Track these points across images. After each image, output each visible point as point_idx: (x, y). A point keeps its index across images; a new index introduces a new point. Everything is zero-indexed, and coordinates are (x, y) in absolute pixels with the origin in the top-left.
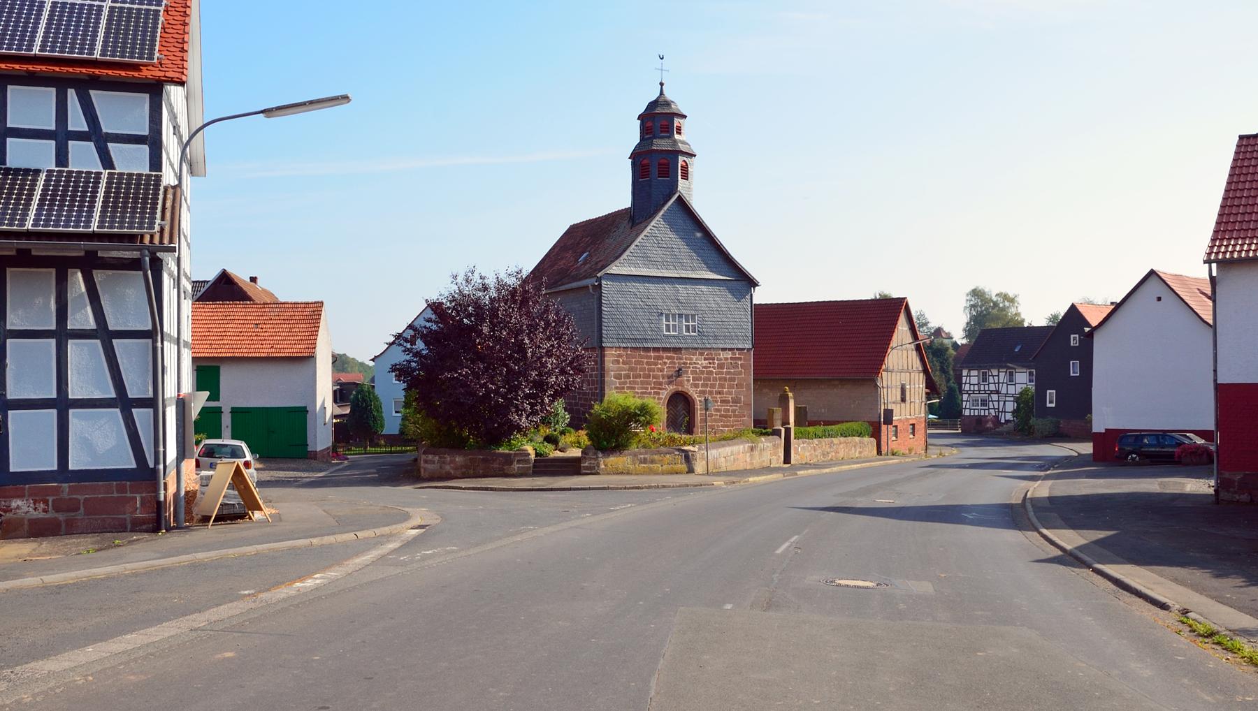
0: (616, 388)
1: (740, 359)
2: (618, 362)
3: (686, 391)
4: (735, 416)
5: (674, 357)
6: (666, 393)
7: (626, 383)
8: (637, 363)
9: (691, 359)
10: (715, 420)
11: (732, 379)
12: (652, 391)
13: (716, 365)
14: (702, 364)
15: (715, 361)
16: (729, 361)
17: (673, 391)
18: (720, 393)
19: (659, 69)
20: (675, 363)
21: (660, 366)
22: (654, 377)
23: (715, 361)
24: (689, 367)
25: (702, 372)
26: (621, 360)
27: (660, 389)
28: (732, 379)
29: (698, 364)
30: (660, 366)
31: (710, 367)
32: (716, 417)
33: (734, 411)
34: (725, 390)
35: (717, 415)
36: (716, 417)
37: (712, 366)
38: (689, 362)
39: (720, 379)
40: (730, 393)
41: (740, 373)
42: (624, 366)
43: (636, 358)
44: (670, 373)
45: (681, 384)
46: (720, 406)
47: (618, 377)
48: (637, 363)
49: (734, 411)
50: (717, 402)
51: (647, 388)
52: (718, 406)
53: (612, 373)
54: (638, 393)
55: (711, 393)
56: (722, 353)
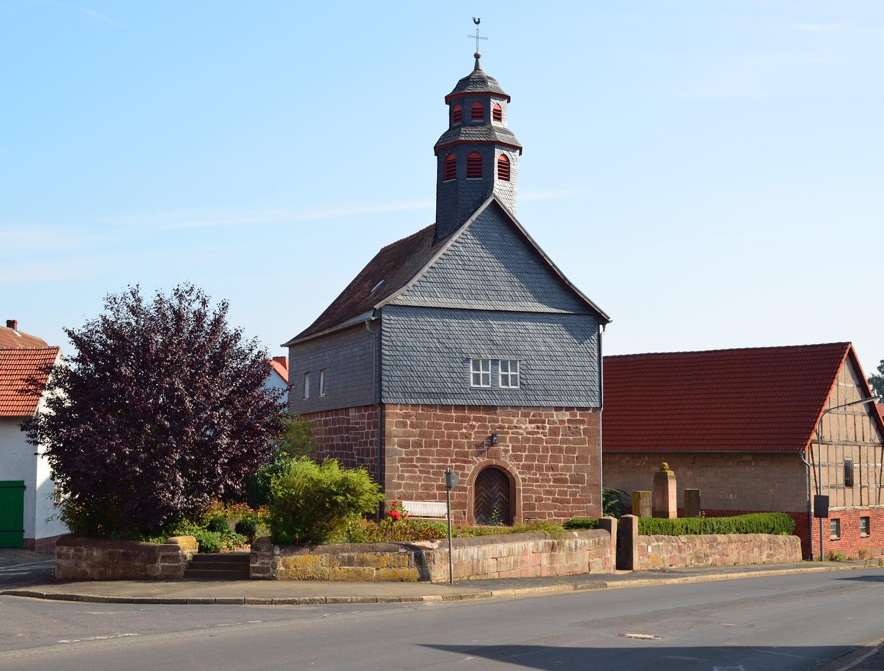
0: (401, 460)
1: (582, 422)
2: (404, 425)
3: (503, 465)
4: (575, 501)
5: (485, 418)
6: (473, 467)
7: (415, 453)
8: (432, 426)
9: (510, 422)
10: (546, 506)
11: (571, 450)
12: (454, 464)
13: (547, 431)
14: (527, 428)
15: (546, 425)
16: (566, 425)
17: (484, 465)
18: (552, 468)
19: (473, 37)
20: (486, 427)
21: (464, 431)
22: (456, 446)
23: (546, 425)
24: (507, 433)
25: (527, 440)
26: (409, 422)
27: (465, 462)
28: (571, 450)
29: (521, 428)
30: (464, 431)
31: (538, 433)
32: (548, 502)
33: (573, 494)
34: (560, 465)
35: (549, 499)
36: (548, 502)
37: (541, 431)
38: (507, 425)
39: (554, 449)
40: (568, 469)
41: (583, 442)
42: (413, 430)
43: (430, 419)
44: (480, 441)
45: (496, 455)
46: (554, 487)
47: (404, 445)
48: (432, 426)
49: (573, 494)
50: (548, 481)
51: (446, 461)
52: (550, 486)
53: (396, 439)
54: (432, 467)
55: (539, 468)
56: (555, 413)
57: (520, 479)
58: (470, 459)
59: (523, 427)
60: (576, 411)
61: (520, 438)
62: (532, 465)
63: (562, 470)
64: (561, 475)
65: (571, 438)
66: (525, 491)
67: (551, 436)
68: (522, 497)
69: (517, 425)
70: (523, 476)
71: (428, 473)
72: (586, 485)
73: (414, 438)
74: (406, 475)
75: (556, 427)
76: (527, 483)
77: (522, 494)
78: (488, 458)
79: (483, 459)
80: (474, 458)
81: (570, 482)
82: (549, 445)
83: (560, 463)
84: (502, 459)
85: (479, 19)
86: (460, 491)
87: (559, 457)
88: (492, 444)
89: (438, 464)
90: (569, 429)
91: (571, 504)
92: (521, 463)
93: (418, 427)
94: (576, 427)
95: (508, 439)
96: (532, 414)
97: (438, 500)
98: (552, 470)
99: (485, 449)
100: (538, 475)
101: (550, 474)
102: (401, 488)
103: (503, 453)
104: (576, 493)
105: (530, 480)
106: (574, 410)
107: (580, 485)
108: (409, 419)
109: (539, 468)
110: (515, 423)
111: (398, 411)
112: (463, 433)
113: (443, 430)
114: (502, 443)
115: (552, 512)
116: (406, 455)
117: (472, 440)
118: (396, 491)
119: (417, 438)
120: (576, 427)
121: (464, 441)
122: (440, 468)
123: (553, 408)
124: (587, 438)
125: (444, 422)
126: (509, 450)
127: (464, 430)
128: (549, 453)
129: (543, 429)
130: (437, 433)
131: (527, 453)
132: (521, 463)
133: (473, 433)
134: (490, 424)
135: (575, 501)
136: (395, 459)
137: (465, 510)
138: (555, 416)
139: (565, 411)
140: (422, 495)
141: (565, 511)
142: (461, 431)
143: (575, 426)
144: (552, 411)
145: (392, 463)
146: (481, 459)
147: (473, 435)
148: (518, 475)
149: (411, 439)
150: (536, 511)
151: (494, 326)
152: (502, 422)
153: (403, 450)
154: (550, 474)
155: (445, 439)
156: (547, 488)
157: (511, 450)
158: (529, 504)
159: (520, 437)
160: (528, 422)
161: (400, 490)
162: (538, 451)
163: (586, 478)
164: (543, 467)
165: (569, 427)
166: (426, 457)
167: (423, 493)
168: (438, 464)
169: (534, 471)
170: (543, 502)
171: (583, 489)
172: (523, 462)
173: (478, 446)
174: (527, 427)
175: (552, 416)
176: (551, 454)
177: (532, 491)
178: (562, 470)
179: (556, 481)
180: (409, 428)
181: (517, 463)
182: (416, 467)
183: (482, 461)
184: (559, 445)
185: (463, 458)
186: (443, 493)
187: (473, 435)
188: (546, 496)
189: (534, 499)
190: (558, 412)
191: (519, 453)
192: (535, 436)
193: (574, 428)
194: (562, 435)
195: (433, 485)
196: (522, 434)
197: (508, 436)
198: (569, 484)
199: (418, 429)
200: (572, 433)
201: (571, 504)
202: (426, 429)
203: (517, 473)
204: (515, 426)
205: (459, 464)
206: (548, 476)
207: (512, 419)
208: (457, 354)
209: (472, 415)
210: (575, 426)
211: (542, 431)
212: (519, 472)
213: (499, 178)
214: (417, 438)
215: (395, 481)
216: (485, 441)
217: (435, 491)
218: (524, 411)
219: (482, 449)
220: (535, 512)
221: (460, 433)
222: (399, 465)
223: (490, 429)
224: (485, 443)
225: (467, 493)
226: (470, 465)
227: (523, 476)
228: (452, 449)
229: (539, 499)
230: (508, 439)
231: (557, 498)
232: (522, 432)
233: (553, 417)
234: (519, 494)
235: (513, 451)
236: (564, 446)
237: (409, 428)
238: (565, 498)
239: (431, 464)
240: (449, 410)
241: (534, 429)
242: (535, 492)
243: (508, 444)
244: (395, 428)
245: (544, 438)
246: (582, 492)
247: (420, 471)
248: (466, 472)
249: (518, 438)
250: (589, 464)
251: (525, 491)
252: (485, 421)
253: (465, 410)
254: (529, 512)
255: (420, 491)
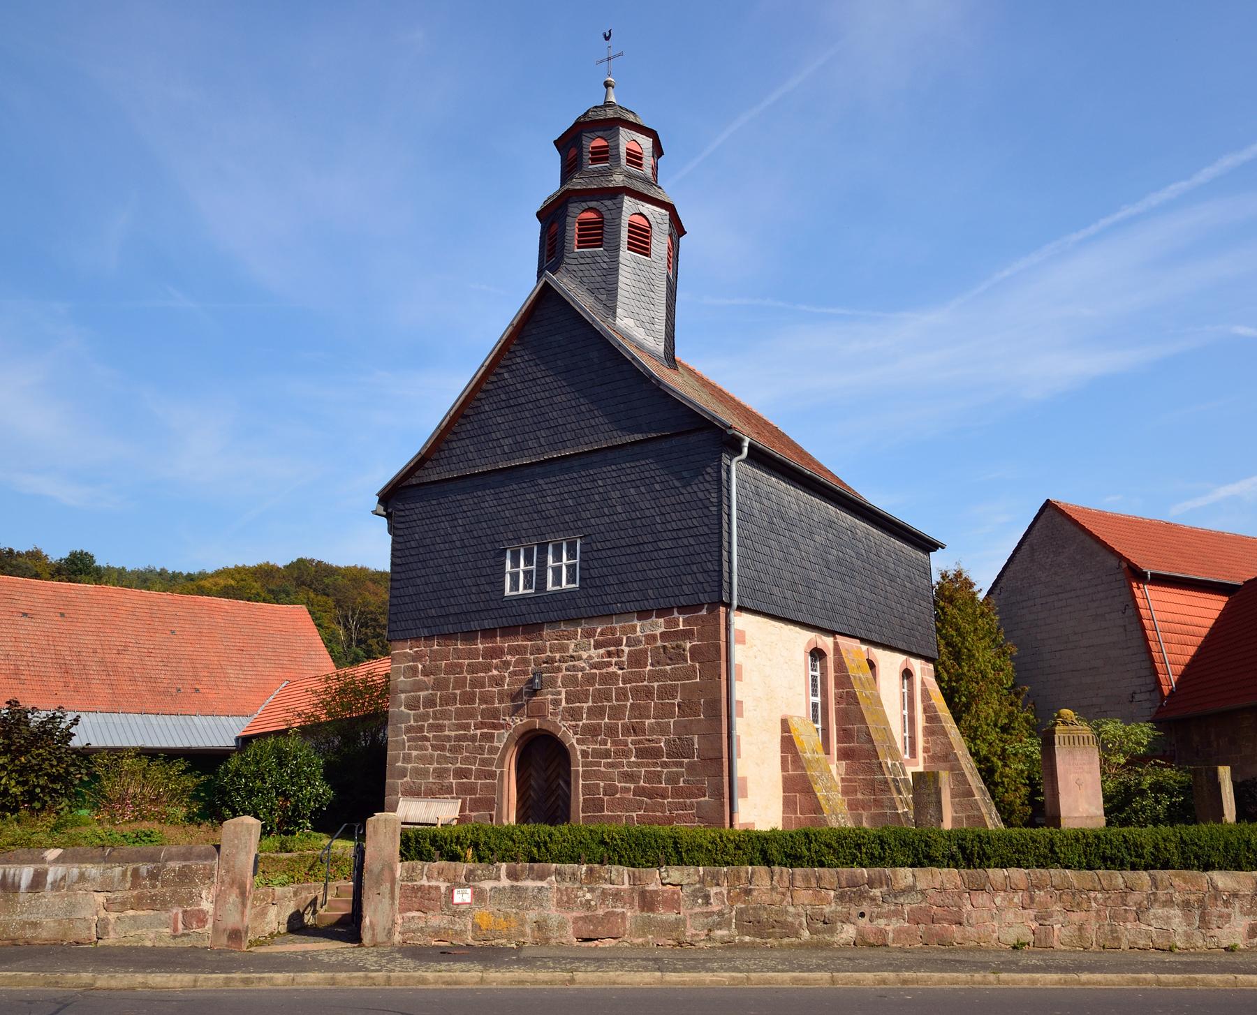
0: (409, 730)
1: (687, 635)
2: (414, 671)
3: (551, 729)
4: (678, 793)
5: (525, 647)
6: (506, 735)
7: (424, 717)
8: (451, 669)
9: (563, 649)
10: (623, 805)
11: (667, 692)
12: (478, 732)
13: (624, 659)
14: (590, 657)
15: (623, 647)
16: (659, 643)
17: (522, 730)
18: (635, 730)
19: (609, 67)
20: (526, 662)
21: (495, 672)
22: (483, 701)
23: (623, 647)
24: (559, 670)
25: (590, 679)
26: (420, 666)
27: (495, 727)
28: (667, 692)
29: (580, 658)
30: (495, 672)
31: (609, 665)
32: (626, 796)
33: (673, 779)
34: (647, 722)
35: (628, 790)
36: (626, 796)
37: (614, 660)
38: (558, 656)
39: (636, 692)
40: (664, 730)
41: (690, 674)
42: (425, 679)
43: (446, 658)
44: (516, 687)
45: (539, 712)
46: (638, 765)
47: (413, 705)
48: (451, 669)
49: (673, 779)
50: (626, 754)
51: (467, 727)
52: (630, 765)
53: (403, 696)
54: (448, 738)
55: (612, 731)
56: (639, 624)
57: (578, 753)
58: (501, 721)
59: (585, 655)
60: (676, 615)
61: (580, 676)
62: (599, 725)
63: (652, 731)
64: (649, 740)
65: (668, 668)
66: (586, 775)
67: (632, 668)
68: (581, 786)
69: (575, 654)
70: (584, 747)
71: (443, 748)
72: (696, 759)
73: (426, 693)
74: (414, 753)
75: (641, 650)
76: (590, 759)
77: (581, 782)
78: (528, 717)
79: (521, 721)
80: (507, 718)
81: (667, 754)
82: (628, 686)
83: (648, 718)
84: (550, 717)
85: (610, 31)
86: (486, 779)
87: (647, 707)
88: (534, 692)
89: (457, 733)
90: (664, 651)
91: (669, 800)
92: (581, 723)
93: (432, 674)
94: (677, 646)
95: (559, 680)
96: (599, 630)
97: (455, 795)
98: (634, 732)
99: (523, 702)
100: (609, 744)
101: (630, 741)
102: (405, 777)
103: (551, 707)
104: (678, 775)
105: (597, 753)
106: (673, 614)
107: (686, 760)
108: (420, 661)
109: (612, 731)
110: (571, 650)
111: (408, 650)
112: (493, 676)
113: (465, 674)
114: (550, 689)
115: (634, 814)
116: (415, 721)
117: (506, 687)
118: (400, 781)
119: (430, 692)
120: (677, 646)
121: (494, 689)
122: (460, 740)
123: (636, 615)
124: (697, 665)
125: (467, 662)
126: (561, 700)
127: (494, 671)
128: (628, 700)
129: (619, 657)
130: (456, 681)
131: (590, 704)
132: (581, 723)
133: (506, 674)
134: (532, 657)
135: (678, 793)
136: (401, 728)
137: (492, 813)
138: (638, 629)
139: (656, 617)
140: (434, 787)
141: (657, 814)
142: (490, 674)
143: (674, 644)
144: (632, 621)
145: (397, 736)
146: (519, 720)
147: (508, 679)
148: (576, 745)
149: (422, 694)
150: (606, 813)
151: (545, 487)
152: (551, 651)
153: (412, 712)
154: (630, 741)
155: (468, 689)
156: (626, 769)
157: (564, 700)
158: (593, 799)
159: (580, 674)
160: (592, 646)
161: (405, 779)
162: (609, 700)
163: (696, 746)
164: (618, 728)
165: (664, 647)
166: (441, 722)
167: (434, 783)
168: (457, 733)
169: (603, 736)
170: (618, 796)
171: (691, 767)
172: (584, 721)
173: (515, 697)
174: (590, 656)
175: (634, 629)
176: (631, 701)
177: (599, 775)
178: (652, 731)
179: (641, 753)
180: (420, 677)
181: (573, 723)
182: (427, 741)
183: (519, 722)
184: (645, 683)
185: (492, 720)
186: (463, 783)
187: (508, 679)
188: (623, 784)
189: (601, 790)
190: (645, 622)
191: (578, 704)
192: (604, 671)
193: (673, 648)
194: (652, 665)
195: (448, 770)
196: (583, 669)
197: (560, 675)
198: (665, 759)
199: (432, 676)
200: (671, 659)
201: (669, 800)
202: (443, 675)
203: (574, 741)
204: (572, 657)
205: (486, 730)
206: (627, 745)
207: (567, 644)
208: (488, 545)
209: (506, 645)
210: (674, 644)
211: (617, 659)
212: (577, 739)
213: (629, 249)
214: (430, 692)
215: (399, 764)
216: (524, 687)
217: (452, 780)
218: (587, 626)
219: (520, 703)
220: (603, 816)
221: (489, 677)
222: (406, 738)
223: (533, 665)
224: (524, 690)
225: (496, 781)
226: (502, 731)
227: (584, 747)
228: (477, 705)
229: (610, 791)
230: (559, 680)
231: (643, 788)
232: (584, 665)
233: (635, 631)
234: (577, 783)
235: (567, 703)
236: (656, 684)
237: (420, 677)
238: (657, 787)
239: (447, 733)
240: (473, 640)
241: (602, 657)
242: (603, 776)
243: (560, 689)
244: (402, 678)
245: (620, 672)
246: (688, 775)
247: (432, 745)
248: (496, 744)
249: (575, 677)
250: (702, 716)
251: (586, 775)
252: (525, 653)
253: (496, 637)
254: (594, 816)
255: (431, 780)
